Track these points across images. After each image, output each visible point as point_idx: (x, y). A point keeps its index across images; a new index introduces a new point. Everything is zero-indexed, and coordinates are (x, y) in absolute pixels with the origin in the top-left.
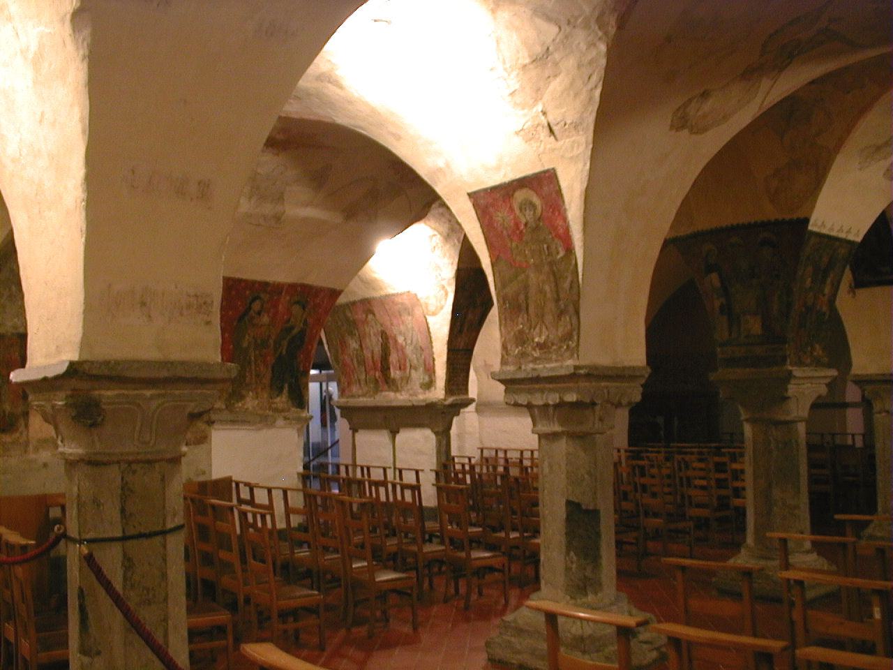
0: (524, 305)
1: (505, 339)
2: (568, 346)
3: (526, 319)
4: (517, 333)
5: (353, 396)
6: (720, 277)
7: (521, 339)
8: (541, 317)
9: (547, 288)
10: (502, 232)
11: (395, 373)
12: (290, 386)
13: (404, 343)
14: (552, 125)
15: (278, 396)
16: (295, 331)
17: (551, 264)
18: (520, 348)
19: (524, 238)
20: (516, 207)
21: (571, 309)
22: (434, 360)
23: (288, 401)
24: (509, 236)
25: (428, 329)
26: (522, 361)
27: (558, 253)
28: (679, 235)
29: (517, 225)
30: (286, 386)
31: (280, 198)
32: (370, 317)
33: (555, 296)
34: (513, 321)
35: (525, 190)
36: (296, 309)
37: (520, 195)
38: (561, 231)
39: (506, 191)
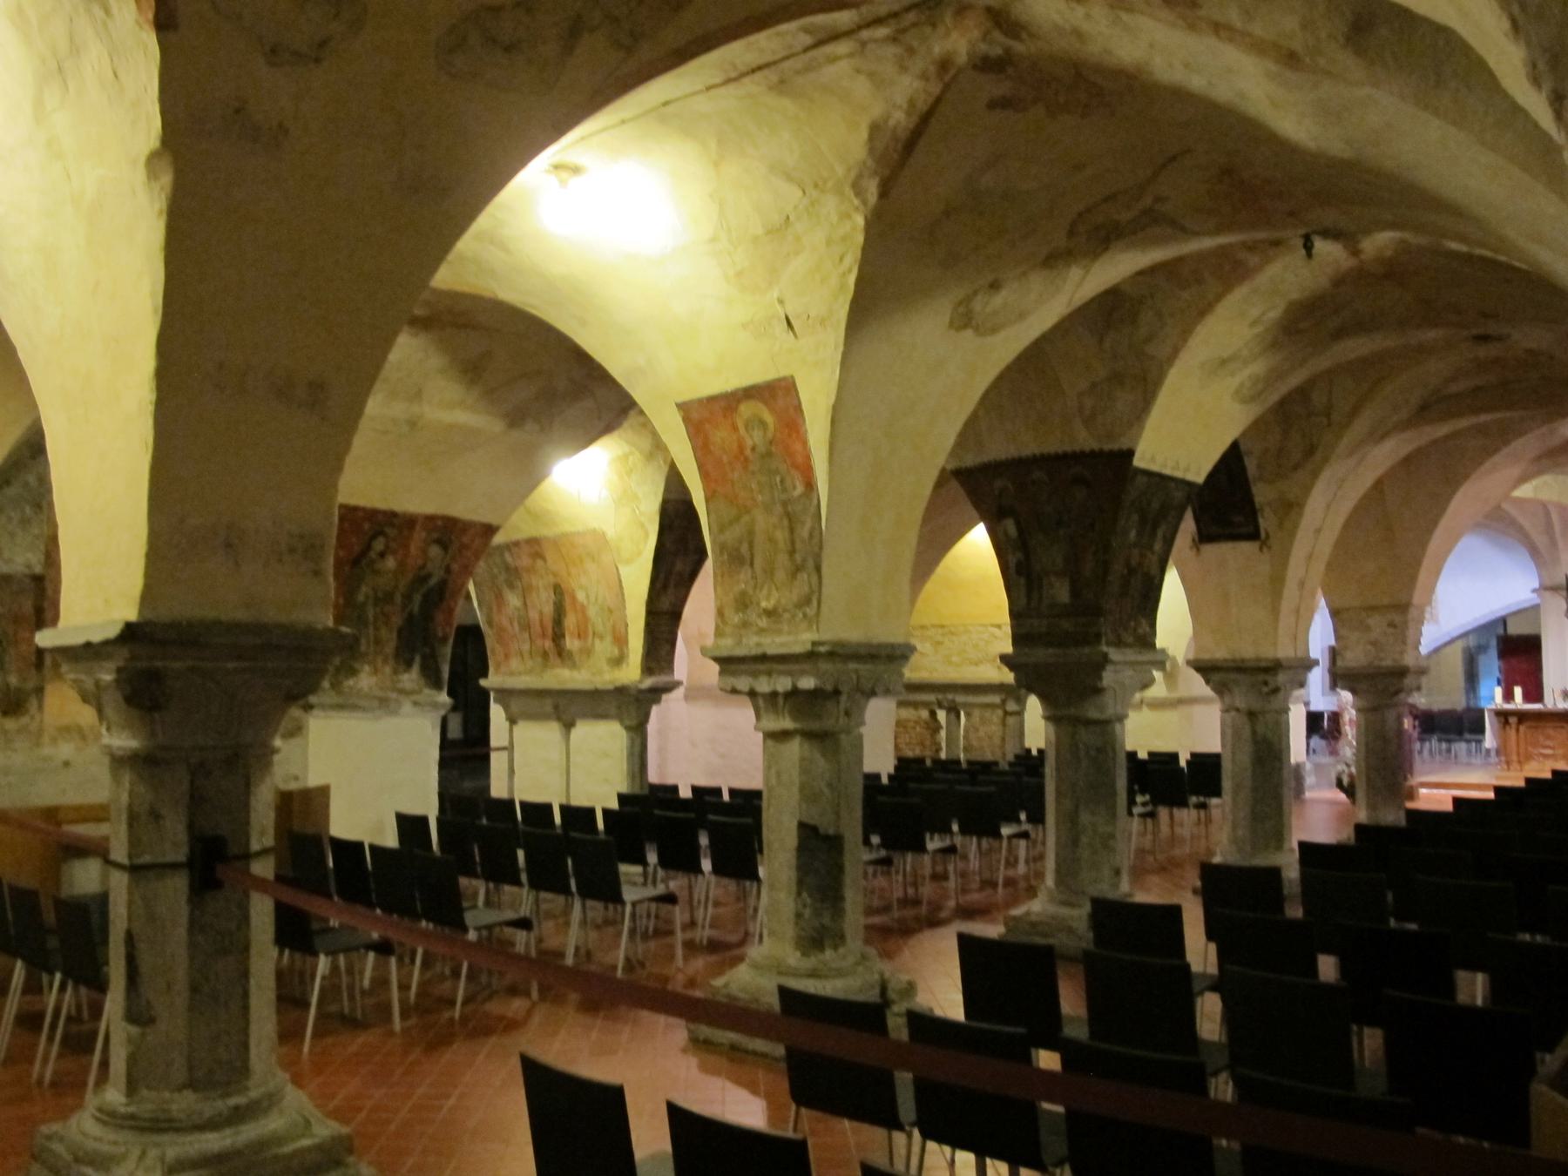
0: (747, 556)
2: (805, 615)
5: (512, 674)
6: (1018, 524)
7: (743, 603)
8: (770, 572)
11: (571, 643)
12: (424, 658)
13: (585, 602)
14: (790, 318)
17: (785, 504)
19: (751, 467)
20: (740, 425)
21: (811, 563)
22: (627, 625)
25: (620, 581)
27: (794, 488)
29: (741, 448)
30: (418, 659)
31: (417, 395)
32: (539, 563)
36: (435, 551)
37: (746, 409)
38: (800, 459)
39: (729, 402)
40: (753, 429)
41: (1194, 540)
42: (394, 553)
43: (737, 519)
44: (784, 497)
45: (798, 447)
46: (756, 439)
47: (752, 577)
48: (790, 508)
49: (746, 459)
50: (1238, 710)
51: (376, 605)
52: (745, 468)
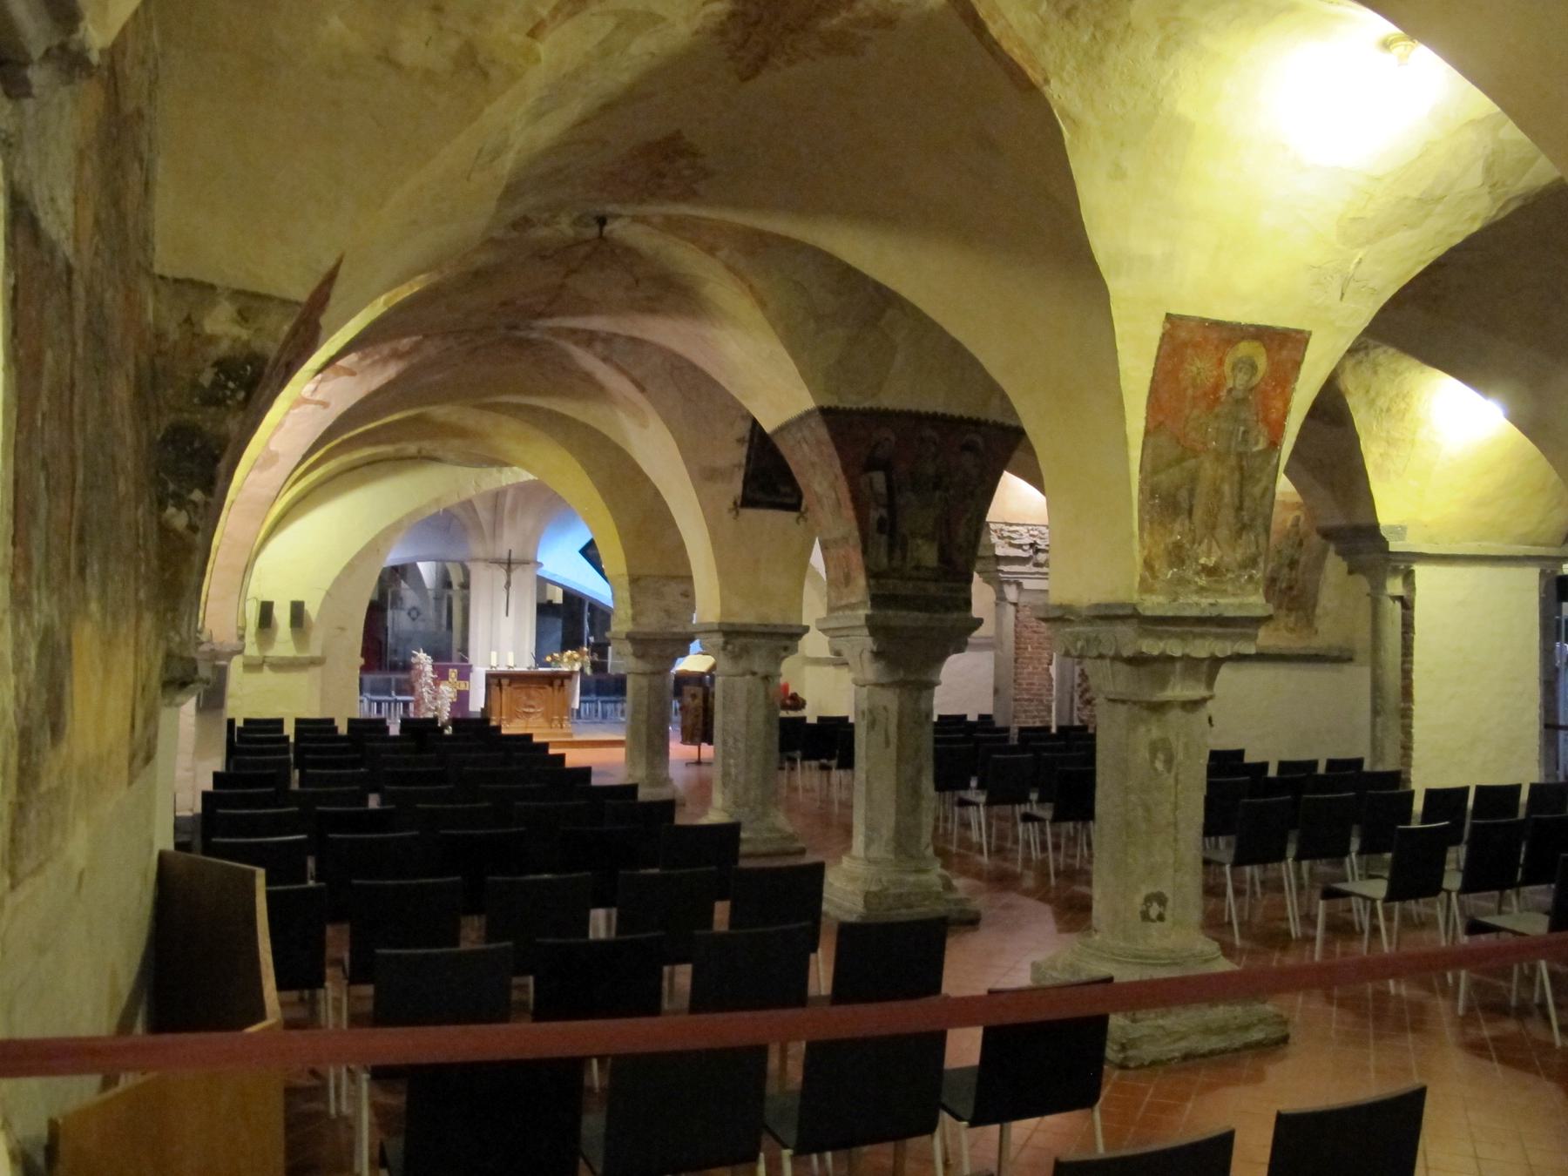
0: (1185, 505)
1: (1150, 552)
2: (1251, 577)
3: (1187, 528)
4: (1170, 547)
6: (889, 480)
7: (1178, 556)
8: (1212, 528)
9: (1226, 488)
10: (1186, 389)
17: (1240, 456)
18: (1175, 570)
19: (1217, 410)
20: (1228, 361)
21: (1259, 522)
24: (1194, 398)
26: (1180, 589)
27: (1257, 443)
28: (841, 405)
29: (1217, 387)
33: (1237, 501)
34: (1166, 528)
35: (1256, 344)
37: (1245, 348)
38: (1274, 416)
39: (1230, 333)
40: (1240, 371)
41: (735, 503)
43: (1180, 460)
44: (1241, 449)
45: (1279, 404)
46: (1238, 382)
47: (1190, 529)
48: (1244, 463)
49: (1217, 399)
50: (754, 674)
52: (1210, 407)
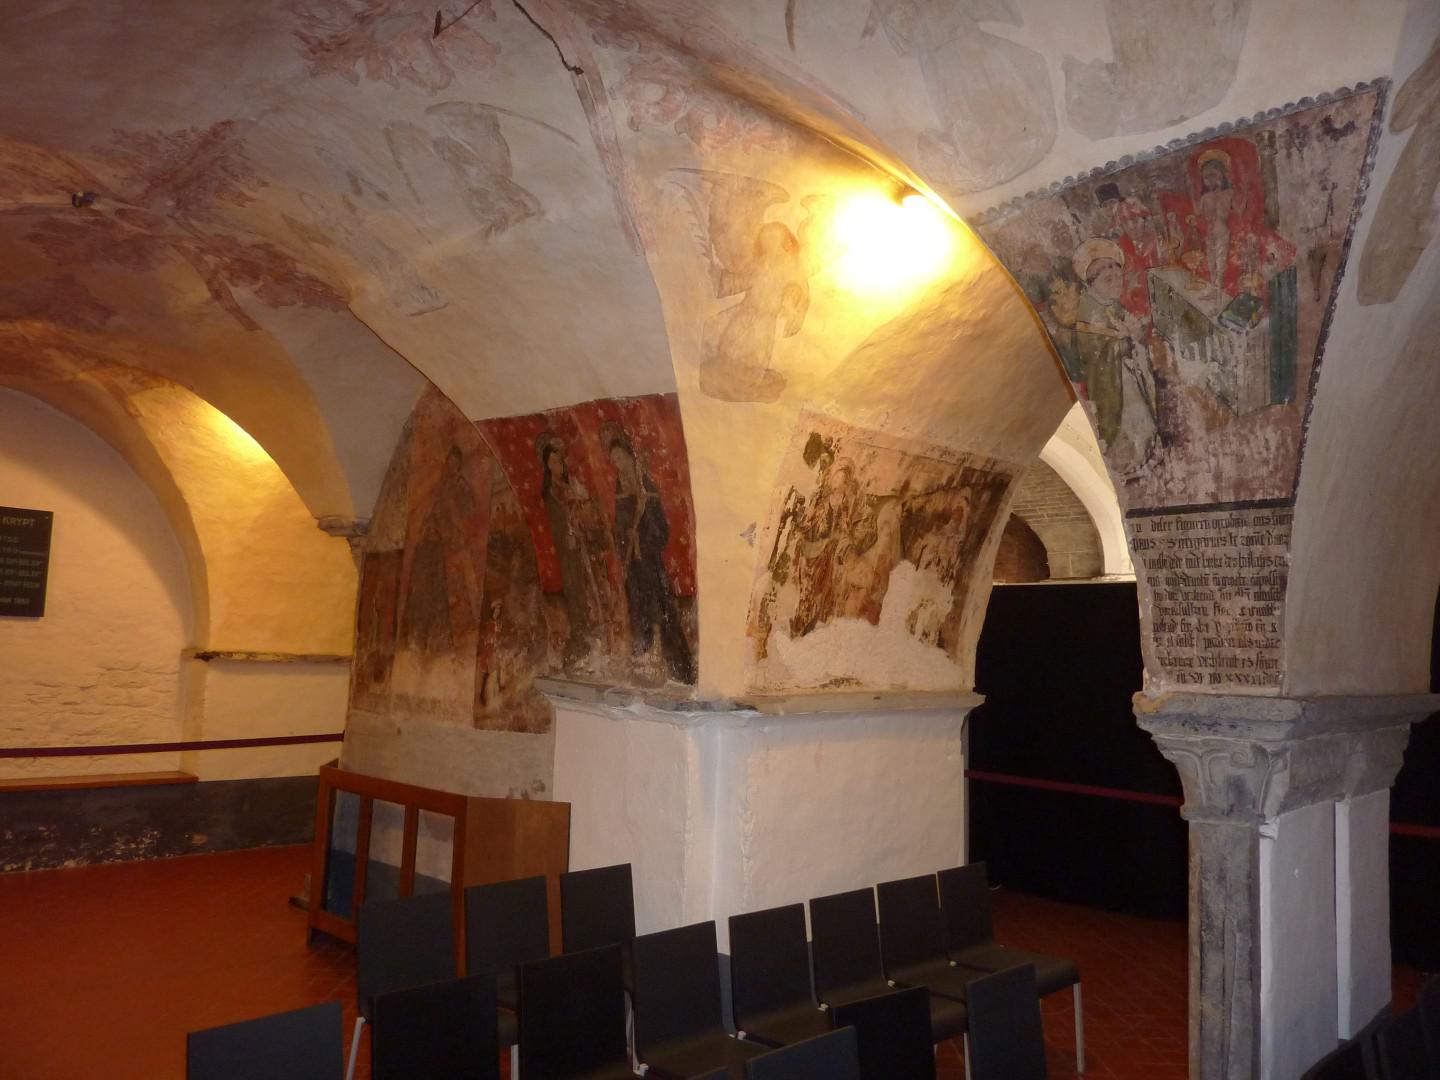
12: (663, 630)
15: (645, 651)
16: (641, 507)
23: (662, 663)
30: (657, 628)
36: (618, 456)
42: (575, 472)
51: (590, 553)
